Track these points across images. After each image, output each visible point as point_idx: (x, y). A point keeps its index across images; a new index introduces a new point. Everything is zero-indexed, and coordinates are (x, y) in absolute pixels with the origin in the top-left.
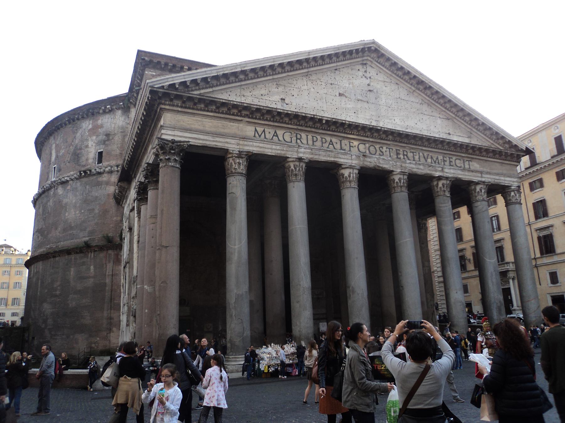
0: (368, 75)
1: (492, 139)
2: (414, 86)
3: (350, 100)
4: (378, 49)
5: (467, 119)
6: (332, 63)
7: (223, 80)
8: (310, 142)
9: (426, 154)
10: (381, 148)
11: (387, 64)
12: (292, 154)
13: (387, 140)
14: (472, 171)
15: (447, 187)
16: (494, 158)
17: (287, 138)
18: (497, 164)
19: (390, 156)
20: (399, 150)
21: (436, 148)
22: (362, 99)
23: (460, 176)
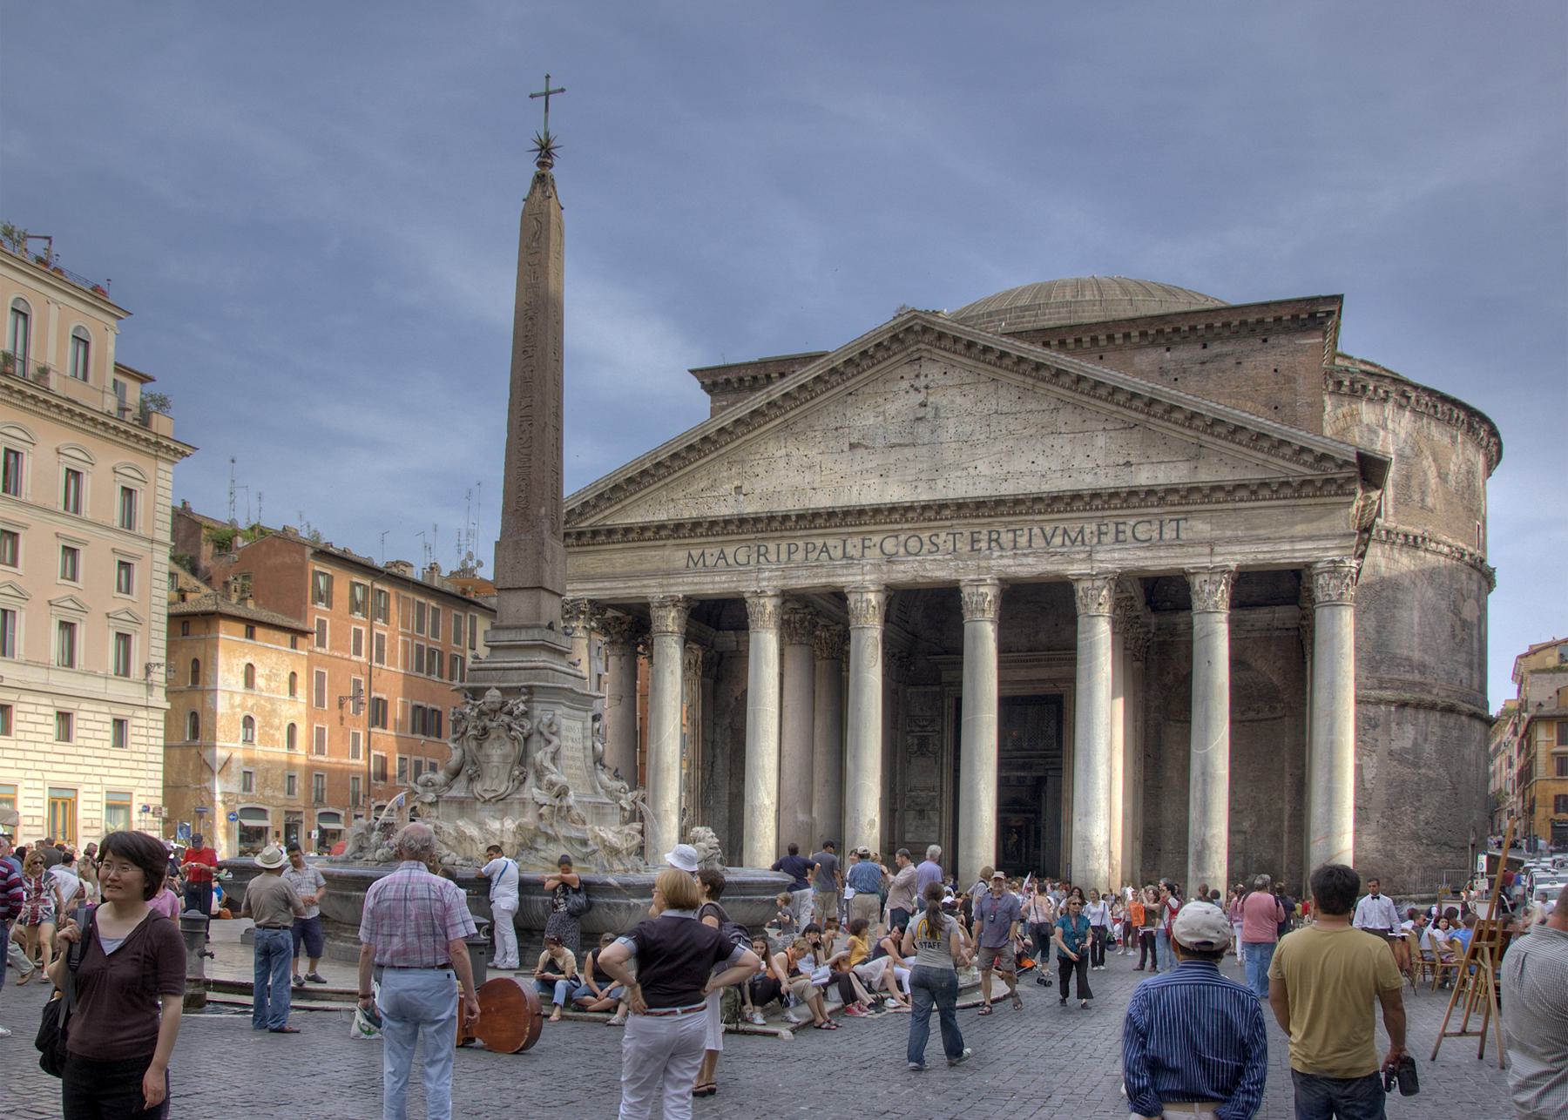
0: (922, 382)
2: (1030, 376)
3: (873, 451)
4: (928, 325)
5: (1176, 415)
6: (833, 387)
8: (784, 557)
9: (1048, 529)
10: (933, 538)
11: (960, 347)
12: (747, 587)
13: (941, 519)
16: (1258, 500)
17: (742, 558)
18: (1276, 511)
19: (955, 550)
20: (979, 532)
21: (1072, 511)
23: (1141, 564)
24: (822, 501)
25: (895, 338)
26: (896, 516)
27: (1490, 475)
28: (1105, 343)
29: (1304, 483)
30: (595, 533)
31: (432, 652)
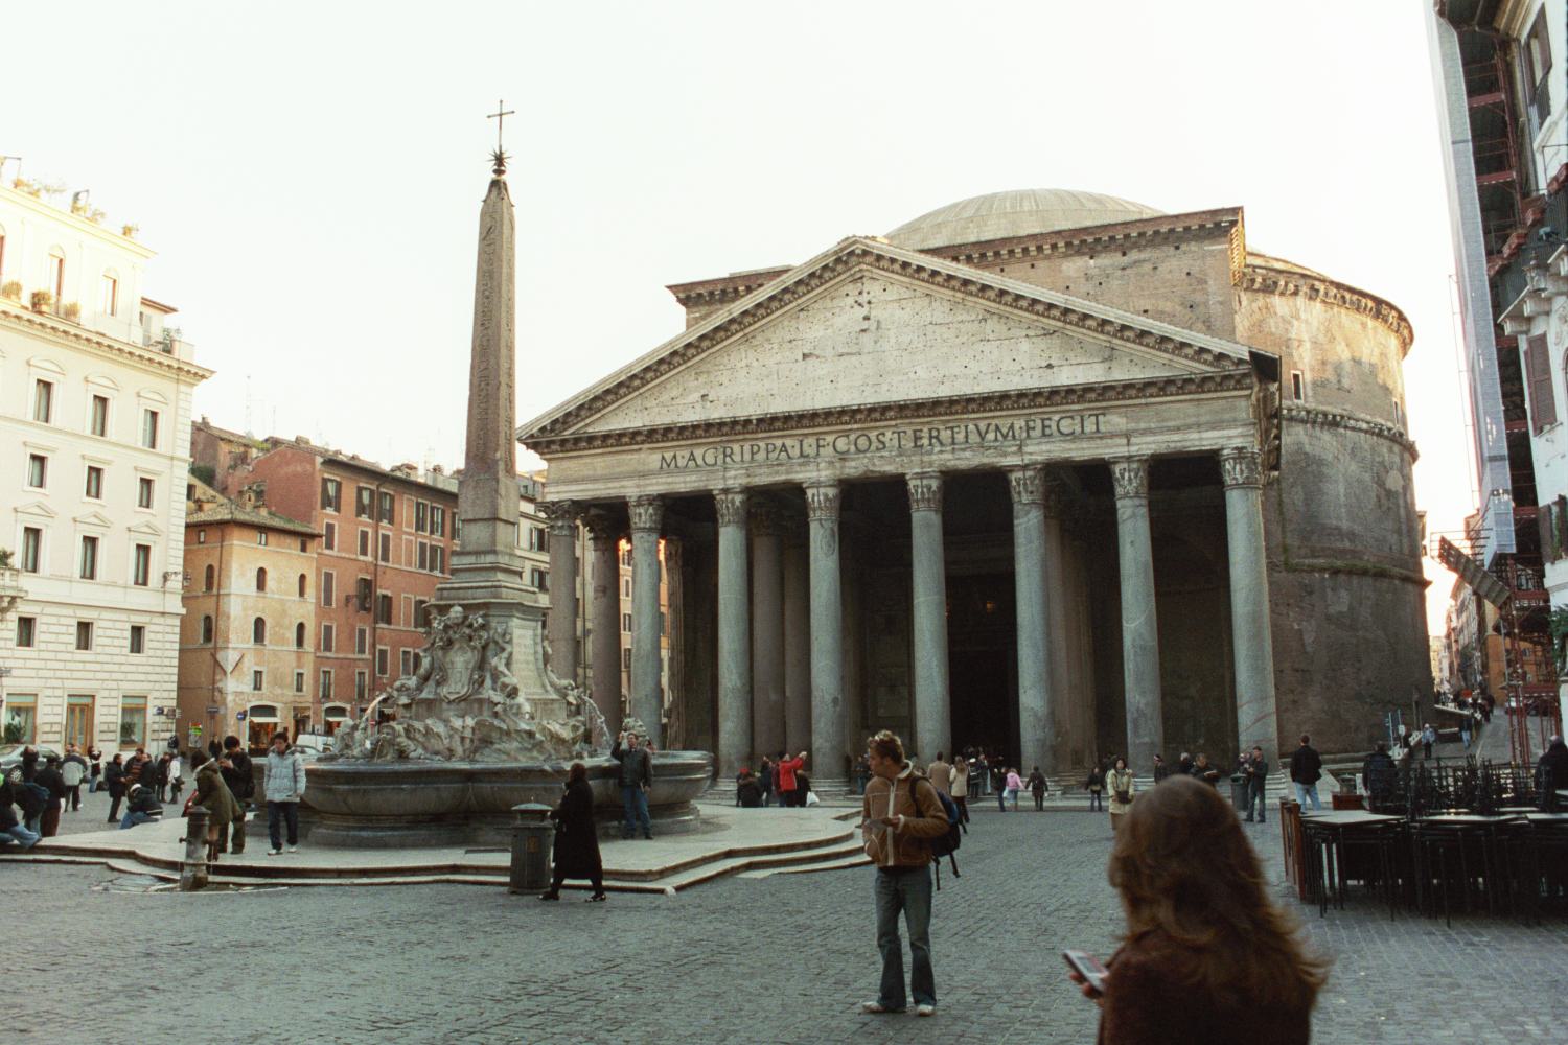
0: (864, 299)
1: (1166, 351)
2: (959, 290)
5: (1090, 322)
6: (786, 304)
7: (610, 398)
8: (747, 456)
9: (982, 425)
11: (897, 267)
12: (716, 485)
13: (886, 420)
14: (1101, 438)
15: (1025, 484)
16: (1166, 395)
17: (710, 459)
21: (1002, 409)
22: (849, 351)
24: (779, 406)
25: (838, 261)
26: (846, 418)
27: (1405, 354)
28: (1035, 253)
29: (1205, 380)
30: (577, 441)
31: (433, 549)
